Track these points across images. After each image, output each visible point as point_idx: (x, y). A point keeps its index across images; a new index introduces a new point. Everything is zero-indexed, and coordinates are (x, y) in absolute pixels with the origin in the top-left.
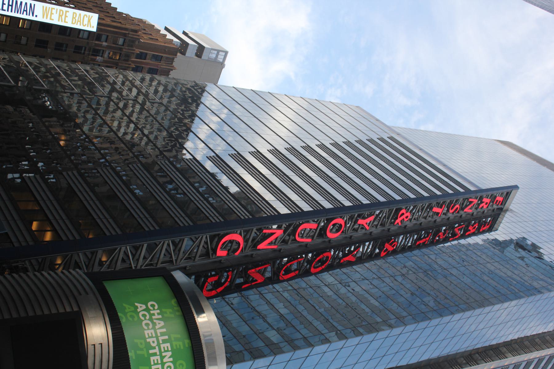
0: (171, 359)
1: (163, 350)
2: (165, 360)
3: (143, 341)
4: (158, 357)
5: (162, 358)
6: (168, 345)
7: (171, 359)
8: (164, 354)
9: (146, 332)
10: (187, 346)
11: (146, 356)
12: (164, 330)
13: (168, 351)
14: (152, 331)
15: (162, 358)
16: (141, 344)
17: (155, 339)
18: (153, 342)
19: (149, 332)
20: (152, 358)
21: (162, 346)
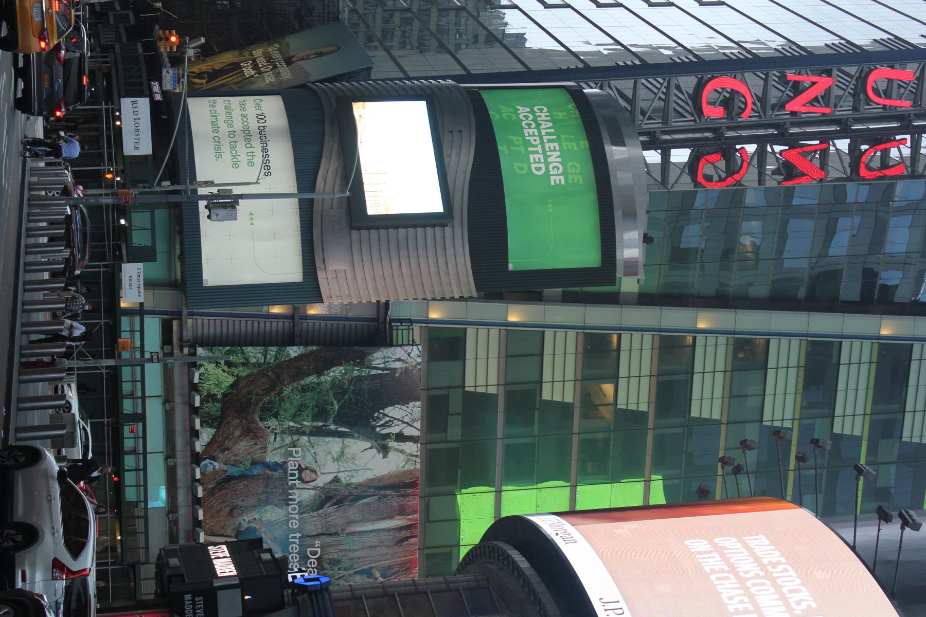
0: (560, 160)
1: (547, 149)
2: (549, 160)
3: (520, 139)
4: (541, 157)
5: (546, 157)
6: (556, 145)
7: (560, 160)
8: (548, 153)
9: (526, 131)
10: (582, 146)
11: (523, 152)
12: (553, 130)
13: (555, 150)
14: (535, 131)
15: (546, 157)
16: (518, 141)
17: (537, 138)
18: (535, 140)
19: (531, 131)
20: (532, 157)
21: (547, 145)
